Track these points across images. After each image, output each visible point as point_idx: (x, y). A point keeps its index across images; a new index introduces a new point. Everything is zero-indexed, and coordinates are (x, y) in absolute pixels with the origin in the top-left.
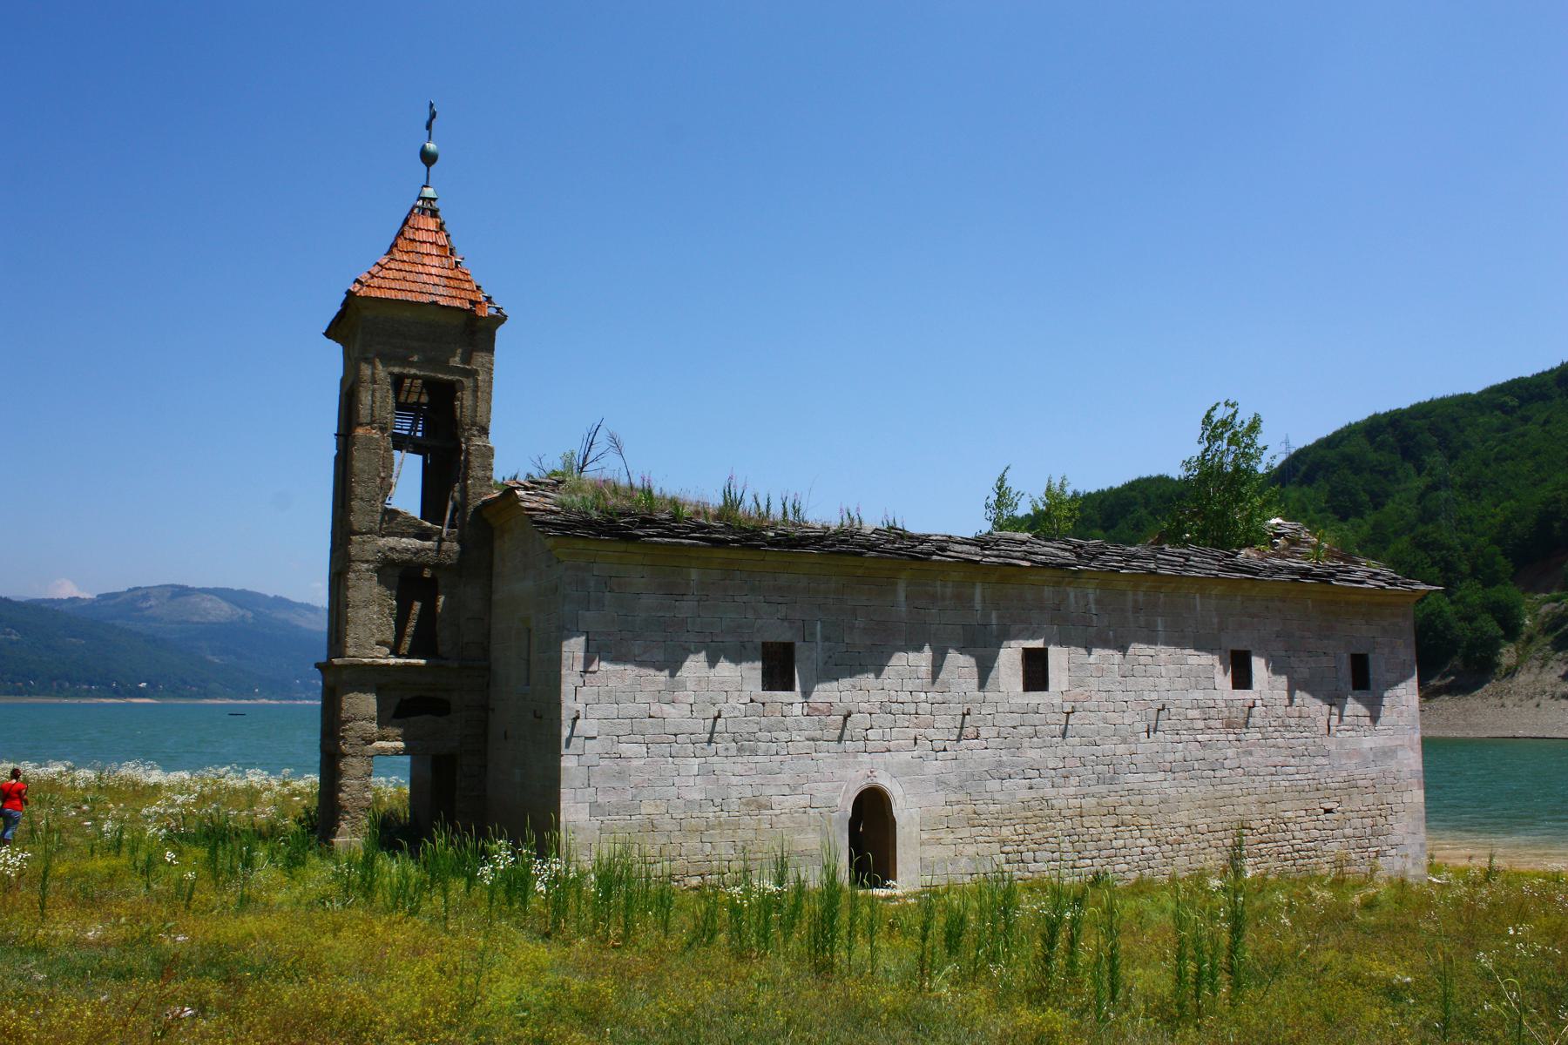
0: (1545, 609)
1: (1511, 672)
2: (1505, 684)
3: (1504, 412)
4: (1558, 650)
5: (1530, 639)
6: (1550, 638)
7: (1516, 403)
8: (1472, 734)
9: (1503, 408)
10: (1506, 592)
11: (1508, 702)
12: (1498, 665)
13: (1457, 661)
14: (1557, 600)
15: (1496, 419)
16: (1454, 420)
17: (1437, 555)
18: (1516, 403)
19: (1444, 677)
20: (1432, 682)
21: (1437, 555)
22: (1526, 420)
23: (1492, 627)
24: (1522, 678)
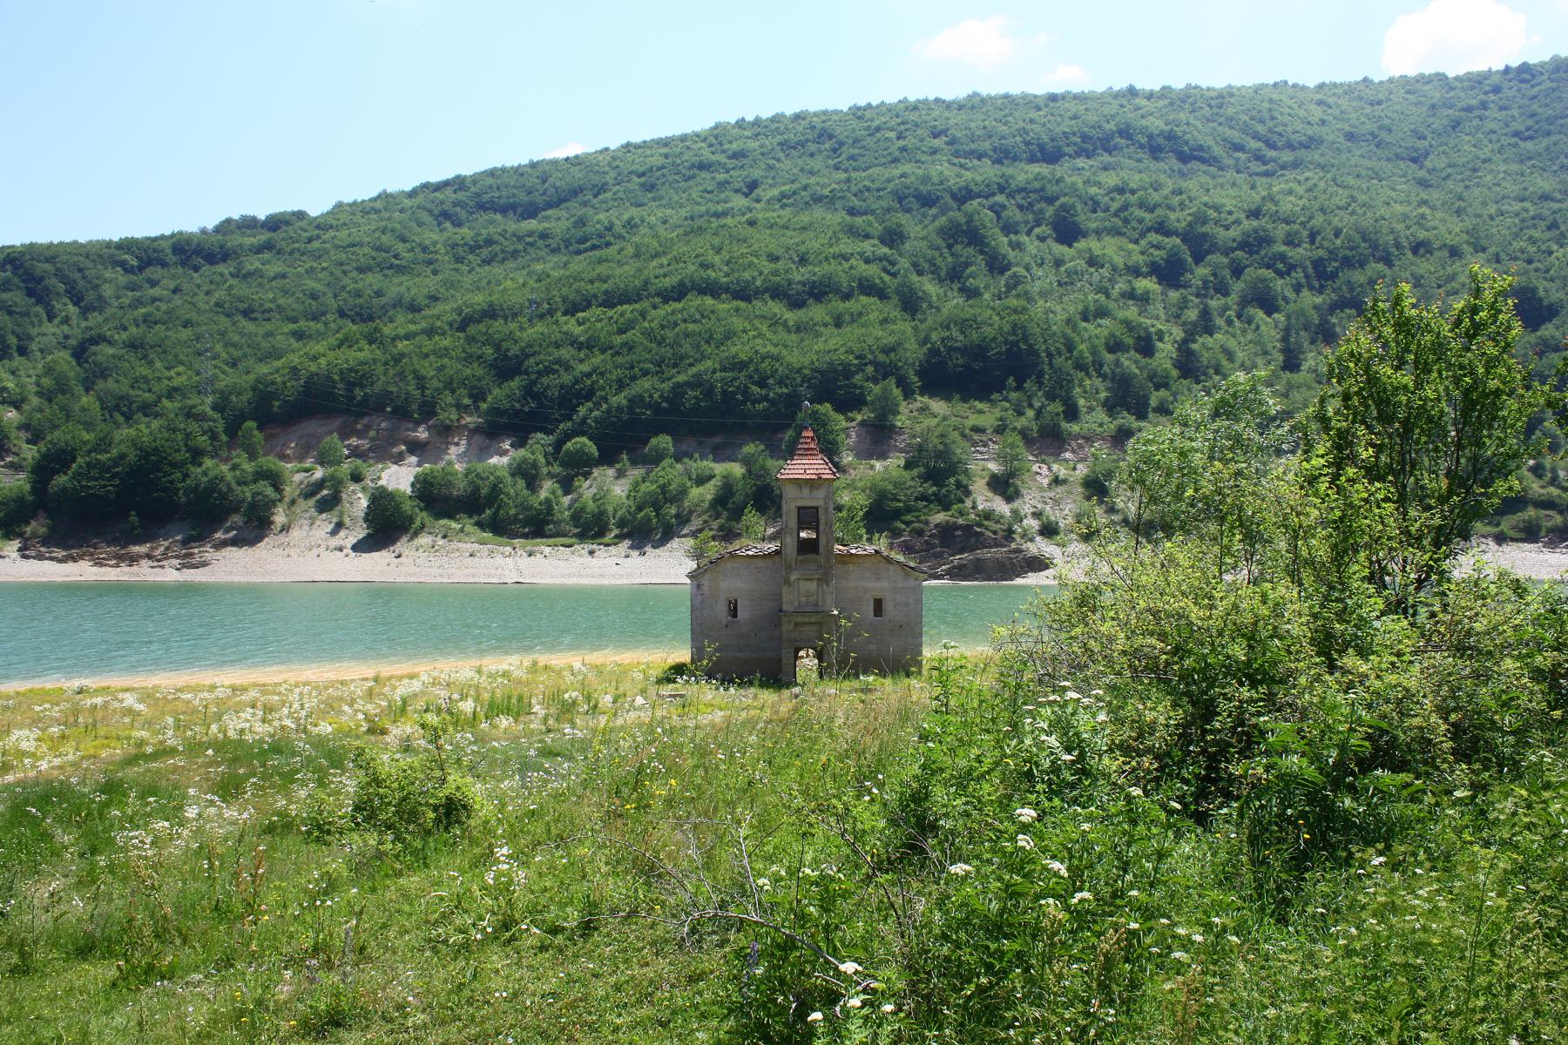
0: (298, 477)
1: (285, 529)
2: (282, 538)
3: (126, 271)
4: (321, 512)
5: (293, 502)
6: (312, 502)
7: (135, 263)
8: (274, 579)
9: (123, 264)
10: (270, 462)
11: (293, 552)
12: (272, 523)
13: (236, 519)
14: (307, 471)
15: (122, 278)
16: (80, 270)
17: (206, 425)
18: (135, 263)
19: (227, 531)
20: (217, 535)
21: (206, 425)
22: (153, 283)
23: (270, 491)
24: (295, 533)
